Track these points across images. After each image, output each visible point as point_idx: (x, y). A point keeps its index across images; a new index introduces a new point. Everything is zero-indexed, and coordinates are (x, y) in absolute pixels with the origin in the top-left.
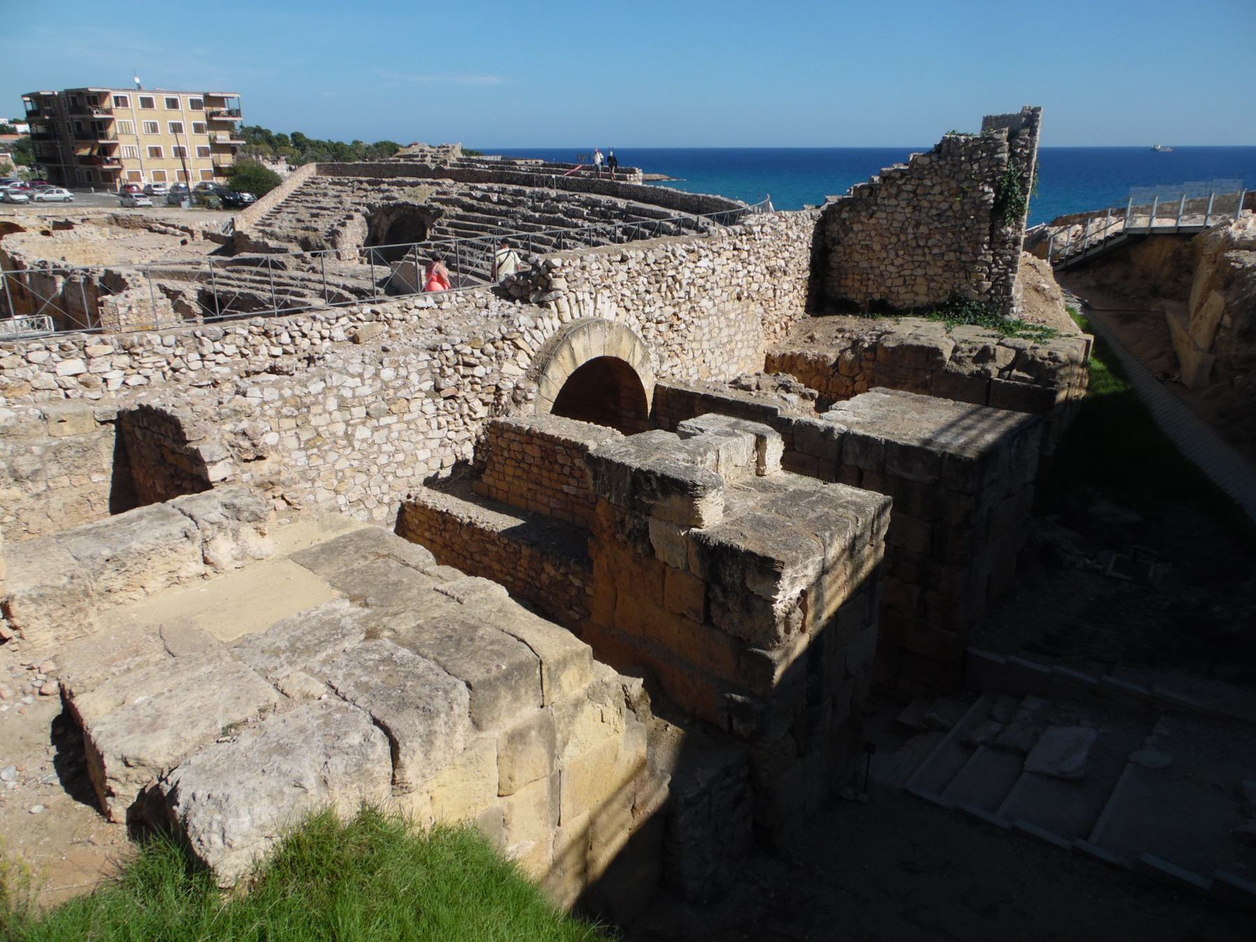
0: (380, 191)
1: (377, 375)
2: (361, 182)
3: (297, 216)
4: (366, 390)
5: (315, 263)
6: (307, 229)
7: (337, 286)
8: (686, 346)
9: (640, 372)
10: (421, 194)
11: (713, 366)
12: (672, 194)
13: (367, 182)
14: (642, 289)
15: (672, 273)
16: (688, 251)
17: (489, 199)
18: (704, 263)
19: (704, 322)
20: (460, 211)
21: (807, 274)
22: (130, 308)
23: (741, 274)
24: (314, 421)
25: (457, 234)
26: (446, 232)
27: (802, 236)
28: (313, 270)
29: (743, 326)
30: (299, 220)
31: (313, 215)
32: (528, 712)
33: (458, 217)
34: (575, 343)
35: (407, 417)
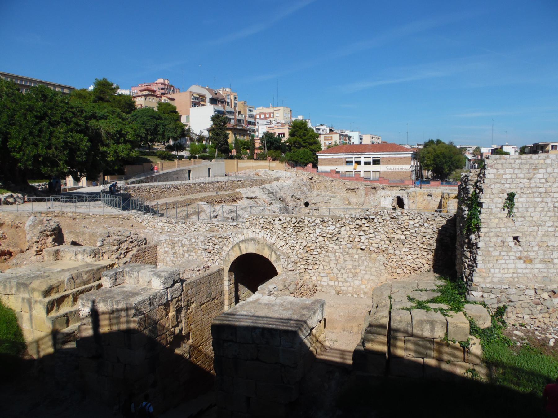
1: (190, 240)
4: (188, 243)
8: (318, 263)
9: (275, 265)
11: (339, 276)
14: (289, 232)
15: (308, 229)
16: (321, 222)
18: (332, 228)
19: (330, 255)
21: (434, 247)
23: (362, 237)
24: (176, 248)
25: (211, 202)
27: (426, 225)
29: (366, 263)
32: (27, 296)
34: (241, 245)
35: (198, 255)
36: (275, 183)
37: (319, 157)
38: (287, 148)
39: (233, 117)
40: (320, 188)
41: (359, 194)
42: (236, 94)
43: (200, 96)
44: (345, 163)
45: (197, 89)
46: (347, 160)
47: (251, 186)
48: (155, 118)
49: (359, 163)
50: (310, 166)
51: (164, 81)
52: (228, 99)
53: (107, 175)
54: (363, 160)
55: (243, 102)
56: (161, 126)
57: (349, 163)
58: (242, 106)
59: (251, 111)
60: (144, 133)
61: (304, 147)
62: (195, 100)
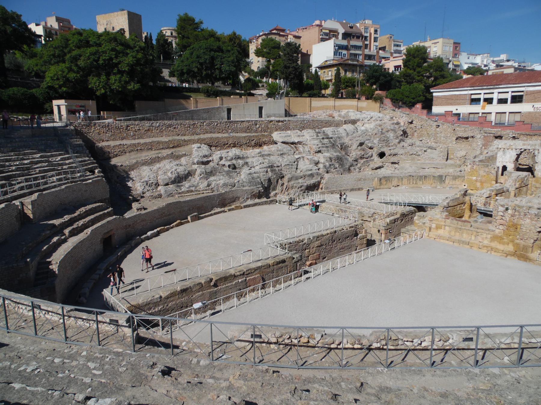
22: (507, 209)
36: (349, 127)
37: (434, 94)
38: (398, 84)
39: (360, 52)
40: (421, 136)
41: (474, 145)
42: (378, 26)
43: (331, 31)
44: (469, 101)
45: (330, 24)
46: (473, 97)
47: (302, 128)
48: (211, 50)
49: (489, 101)
50: (419, 106)
51: (321, 23)
52: (367, 32)
53: (103, 110)
54: (495, 97)
55: (388, 36)
56: (219, 59)
57: (475, 101)
58: (388, 40)
59: (397, 46)
60: (197, 67)
61: (419, 81)
62: (324, 37)
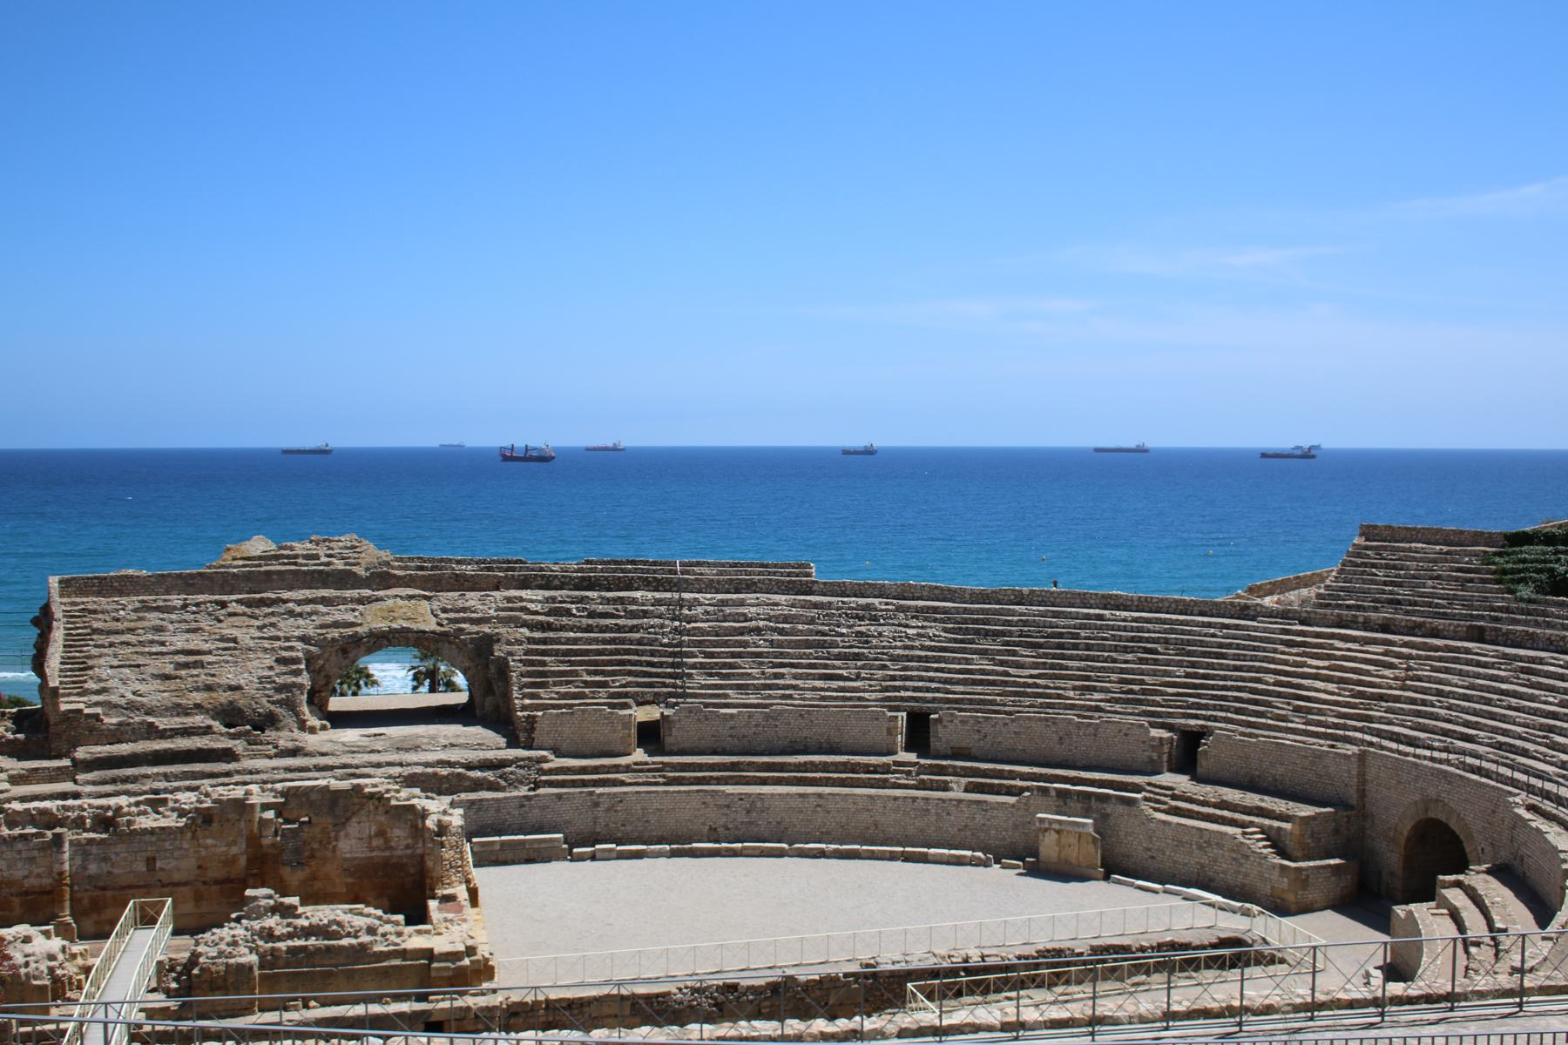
0: (291, 613)
2: (223, 605)
3: (150, 670)
5: (284, 739)
6: (209, 688)
7: (427, 765)
10: (424, 615)
12: (949, 590)
13: (238, 601)
17: (568, 613)
20: (525, 631)
26: (544, 664)
28: (294, 752)
30: (167, 677)
31: (186, 666)
33: (531, 640)
